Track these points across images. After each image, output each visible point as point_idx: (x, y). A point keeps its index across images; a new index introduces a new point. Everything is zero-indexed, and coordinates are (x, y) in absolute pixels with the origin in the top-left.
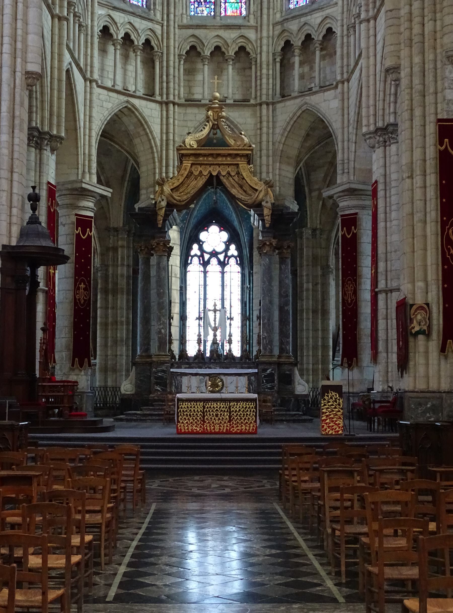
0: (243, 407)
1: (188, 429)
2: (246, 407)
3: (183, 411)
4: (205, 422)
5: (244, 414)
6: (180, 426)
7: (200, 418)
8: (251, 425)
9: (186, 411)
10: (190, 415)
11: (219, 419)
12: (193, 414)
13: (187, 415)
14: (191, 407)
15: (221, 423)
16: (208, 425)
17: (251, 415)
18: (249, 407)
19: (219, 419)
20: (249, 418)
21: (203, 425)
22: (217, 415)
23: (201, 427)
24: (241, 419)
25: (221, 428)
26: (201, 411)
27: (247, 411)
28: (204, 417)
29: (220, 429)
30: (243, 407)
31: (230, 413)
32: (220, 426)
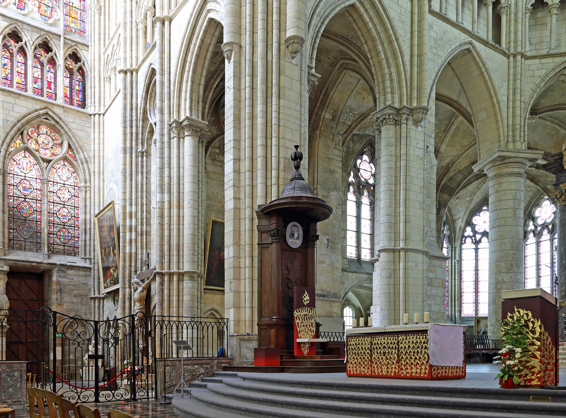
0: (413, 342)
1: (356, 371)
2: (417, 342)
3: (352, 348)
4: (372, 362)
5: (414, 352)
6: (350, 367)
7: (368, 358)
8: (423, 367)
9: (355, 349)
10: (358, 353)
11: (387, 358)
12: (361, 353)
13: (355, 353)
14: (359, 344)
15: (389, 363)
16: (375, 366)
17: (423, 352)
18: (421, 342)
19: (387, 358)
20: (420, 358)
21: (371, 366)
22: (384, 353)
23: (368, 368)
24: (411, 358)
25: (389, 370)
26: (368, 348)
27: (418, 347)
28: (371, 356)
29: (388, 372)
30: (413, 342)
31: (399, 351)
32: (388, 368)
